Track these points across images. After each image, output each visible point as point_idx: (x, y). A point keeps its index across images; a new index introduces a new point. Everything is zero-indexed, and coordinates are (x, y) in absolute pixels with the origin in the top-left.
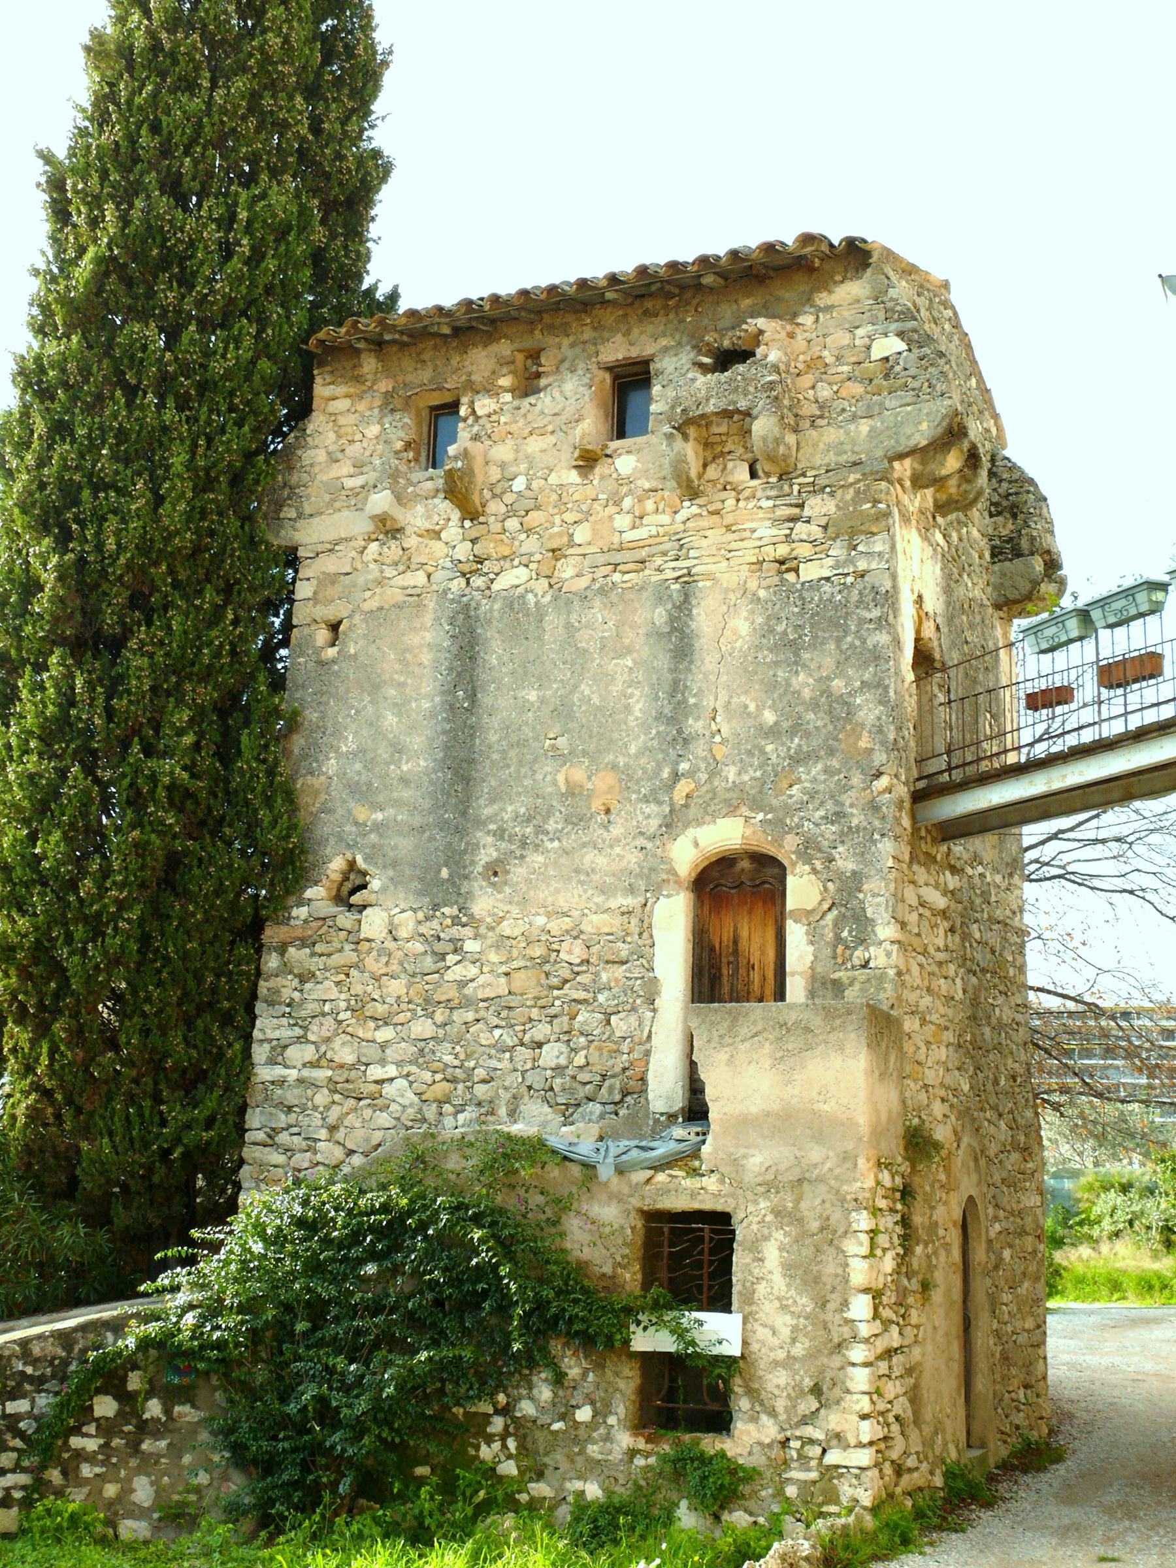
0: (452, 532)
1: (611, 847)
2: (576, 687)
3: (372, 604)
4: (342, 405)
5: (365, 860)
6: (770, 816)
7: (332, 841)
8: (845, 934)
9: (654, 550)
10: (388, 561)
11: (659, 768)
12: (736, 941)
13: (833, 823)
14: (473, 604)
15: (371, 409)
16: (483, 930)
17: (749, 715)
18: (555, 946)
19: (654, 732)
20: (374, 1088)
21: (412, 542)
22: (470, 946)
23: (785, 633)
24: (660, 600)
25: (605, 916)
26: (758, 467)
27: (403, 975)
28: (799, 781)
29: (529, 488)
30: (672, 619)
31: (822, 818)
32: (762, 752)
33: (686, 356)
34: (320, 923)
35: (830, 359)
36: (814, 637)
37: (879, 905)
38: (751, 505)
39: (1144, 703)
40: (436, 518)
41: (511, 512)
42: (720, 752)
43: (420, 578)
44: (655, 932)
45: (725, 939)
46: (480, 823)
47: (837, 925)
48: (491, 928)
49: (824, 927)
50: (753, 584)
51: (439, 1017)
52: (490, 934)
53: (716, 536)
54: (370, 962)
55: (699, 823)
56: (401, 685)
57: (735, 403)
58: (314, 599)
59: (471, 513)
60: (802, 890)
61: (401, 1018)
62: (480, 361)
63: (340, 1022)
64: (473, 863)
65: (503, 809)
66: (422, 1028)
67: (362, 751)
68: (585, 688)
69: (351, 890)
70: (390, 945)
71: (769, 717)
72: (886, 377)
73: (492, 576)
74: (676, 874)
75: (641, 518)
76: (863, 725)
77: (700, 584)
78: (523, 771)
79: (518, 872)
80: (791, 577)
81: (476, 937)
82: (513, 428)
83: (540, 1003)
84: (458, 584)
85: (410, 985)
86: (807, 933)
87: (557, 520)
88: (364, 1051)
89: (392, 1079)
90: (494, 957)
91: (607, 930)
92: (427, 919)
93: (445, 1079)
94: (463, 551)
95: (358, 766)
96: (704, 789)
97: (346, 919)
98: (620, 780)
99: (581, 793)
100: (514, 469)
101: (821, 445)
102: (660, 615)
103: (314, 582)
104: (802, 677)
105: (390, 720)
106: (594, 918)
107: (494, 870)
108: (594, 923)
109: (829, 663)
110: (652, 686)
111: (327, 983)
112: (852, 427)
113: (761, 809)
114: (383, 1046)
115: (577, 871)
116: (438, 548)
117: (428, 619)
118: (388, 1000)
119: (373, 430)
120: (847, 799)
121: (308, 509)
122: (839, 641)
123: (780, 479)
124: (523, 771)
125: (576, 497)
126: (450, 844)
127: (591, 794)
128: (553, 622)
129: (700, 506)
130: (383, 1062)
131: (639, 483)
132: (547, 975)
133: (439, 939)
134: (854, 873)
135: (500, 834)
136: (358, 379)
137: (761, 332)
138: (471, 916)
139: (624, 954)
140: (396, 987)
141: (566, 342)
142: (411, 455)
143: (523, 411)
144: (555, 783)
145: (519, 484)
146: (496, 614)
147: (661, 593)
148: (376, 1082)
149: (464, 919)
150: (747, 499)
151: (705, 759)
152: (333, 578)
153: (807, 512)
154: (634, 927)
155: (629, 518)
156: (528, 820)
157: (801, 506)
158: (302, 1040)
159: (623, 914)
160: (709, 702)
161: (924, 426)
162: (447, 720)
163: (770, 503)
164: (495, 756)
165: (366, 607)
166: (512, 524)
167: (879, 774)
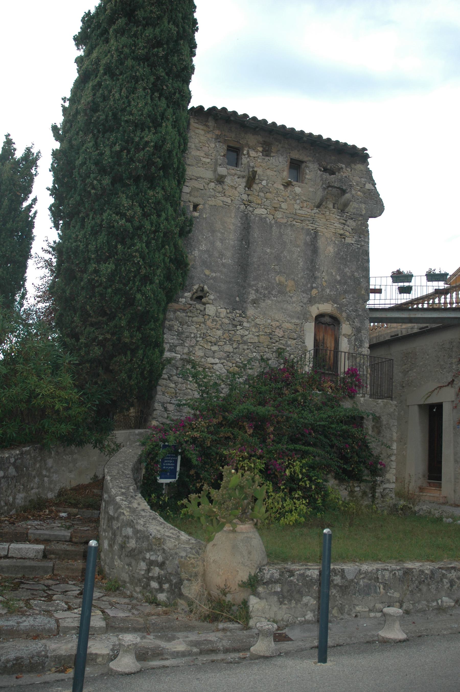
7: (196, 279)
9: (306, 219)
10: (217, 191)
12: (323, 339)
21: (226, 187)
22: (245, 324)
28: (346, 298)
29: (267, 185)
30: (312, 241)
33: (316, 166)
36: (350, 259)
41: (261, 190)
42: (324, 284)
46: (250, 286)
47: (356, 340)
50: (334, 239)
51: (235, 346)
53: (323, 220)
54: (209, 323)
55: (319, 303)
58: (190, 193)
60: (346, 328)
62: (252, 139)
63: (197, 341)
64: (247, 298)
66: (228, 348)
68: (285, 253)
69: (200, 297)
72: (369, 194)
79: (263, 305)
80: (343, 240)
81: (248, 322)
84: (243, 207)
85: (224, 334)
89: (216, 364)
90: (254, 330)
92: (230, 312)
97: (199, 306)
102: (308, 238)
105: (218, 244)
106: (286, 324)
107: (254, 302)
108: (286, 325)
110: (306, 259)
111: (193, 327)
114: (214, 352)
115: (282, 308)
117: (233, 215)
127: (286, 286)
130: (214, 358)
131: (302, 197)
132: (271, 338)
133: (234, 319)
135: (257, 291)
136: (207, 126)
137: (342, 168)
138: (246, 315)
139: (296, 337)
143: (266, 160)
144: (275, 279)
145: (264, 183)
147: (308, 232)
148: (211, 364)
158: (182, 345)
160: (322, 268)
162: (240, 250)
163: (339, 217)
164: (255, 266)
165: (210, 203)
166: (262, 194)
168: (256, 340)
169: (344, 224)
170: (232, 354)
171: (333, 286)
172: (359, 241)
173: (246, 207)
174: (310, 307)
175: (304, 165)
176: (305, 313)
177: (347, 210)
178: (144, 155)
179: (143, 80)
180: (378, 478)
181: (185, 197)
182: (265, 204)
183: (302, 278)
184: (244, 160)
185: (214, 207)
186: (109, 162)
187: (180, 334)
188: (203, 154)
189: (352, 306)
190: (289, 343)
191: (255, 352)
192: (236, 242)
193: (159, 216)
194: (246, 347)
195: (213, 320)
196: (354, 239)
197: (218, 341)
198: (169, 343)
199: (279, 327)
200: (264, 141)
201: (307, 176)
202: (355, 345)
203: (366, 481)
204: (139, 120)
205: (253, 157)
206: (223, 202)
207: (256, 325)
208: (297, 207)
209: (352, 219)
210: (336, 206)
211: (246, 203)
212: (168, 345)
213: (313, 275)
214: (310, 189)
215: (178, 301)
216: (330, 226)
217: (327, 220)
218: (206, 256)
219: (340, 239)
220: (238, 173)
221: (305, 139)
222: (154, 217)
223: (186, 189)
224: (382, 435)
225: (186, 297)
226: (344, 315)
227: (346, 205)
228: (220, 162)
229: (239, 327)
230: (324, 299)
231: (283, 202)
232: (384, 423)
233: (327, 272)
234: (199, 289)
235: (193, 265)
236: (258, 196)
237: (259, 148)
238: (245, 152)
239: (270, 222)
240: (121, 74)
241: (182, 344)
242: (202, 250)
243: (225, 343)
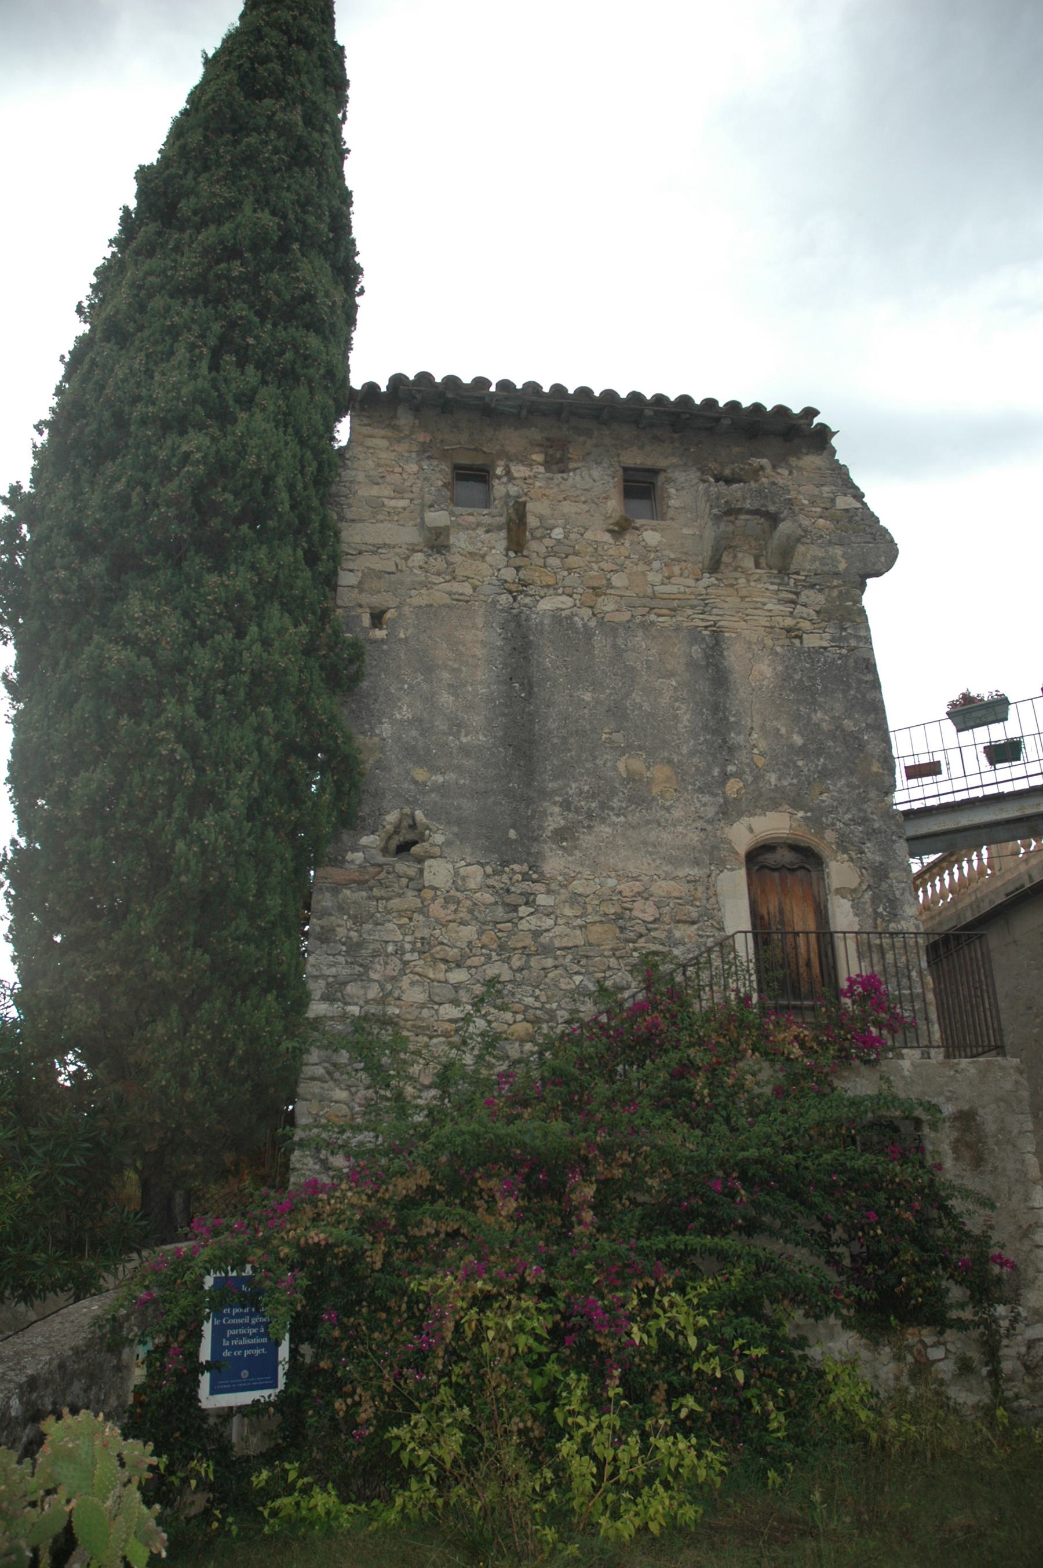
1: (675, 826)
3: (416, 601)
5: (426, 815)
7: (389, 796)
8: (880, 910)
9: (683, 603)
12: (781, 911)
13: (859, 824)
20: (448, 1026)
21: (457, 559)
22: (542, 900)
23: (801, 681)
27: (474, 922)
28: (828, 790)
30: (707, 657)
32: (795, 763)
33: (694, 475)
34: (377, 869)
36: (825, 687)
37: (904, 889)
39: (1010, 778)
40: (480, 545)
41: (551, 552)
42: (761, 762)
43: (467, 589)
44: (720, 898)
45: (771, 909)
46: (544, 794)
47: (875, 900)
50: (769, 642)
51: (516, 962)
53: (733, 601)
54: (436, 909)
56: (455, 671)
58: (360, 587)
59: (517, 544)
60: (840, 872)
61: (475, 961)
62: (512, 439)
63: (406, 963)
64: (541, 828)
68: (636, 697)
72: (850, 521)
74: (737, 853)
75: (669, 578)
79: (587, 840)
80: (797, 642)
81: (549, 892)
82: (547, 492)
83: (618, 953)
84: (505, 599)
85: (481, 933)
86: (852, 907)
88: (437, 990)
90: (568, 912)
91: (676, 894)
92: (495, 873)
93: (525, 1020)
97: (405, 867)
98: (677, 773)
99: (640, 780)
102: (696, 651)
103: (360, 574)
104: (819, 714)
105: (446, 699)
106: (663, 883)
107: (561, 835)
108: (661, 888)
111: (390, 926)
113: (801, 808)
114: (457, 987)
115: (645, 843)
116: (484, 567)
117: (480, 621)
121: (349, 514)
123: (780, 572)
127: (650, 781)
128: (600, 643)
131: (666, 553)
132: (622, 929)
133: (508, 891)
134: (881, 864)
135: (566, 805)
136: (395, 428)
138: (542, 874)
139: (694, 915)
140: (469, 932)
143: (555, 481)
144: (615, 768)
145: (558, 533)
147: (694, 636)
149: (535, 876)
151: (748, 765)
152: (380, 574)
153: (803, 598)
157: (797, 594)
158: (362, 978)
163: (776, 587)
164: (555, 740)
166: (554, 562)
168: (578, 938)
169: (794, 602)
170: (509, 987)
171: (785, 764)
172: (841, 638)
173: (515, 599)
174: (726, 830)
175: (661, 478)
176: (714, 847)
177: (793, 568)
178: (180, 487)
179: (189, 330)
180: (1001, 1310)
181: (345, 597)
182: (567, 582)
183: (692, 754)
184: (499, 489)
185: (429, 610)
186: (98, 522)
187: (354, 948)
188: (387, 491)
190: (677, 934)
191: (577, 973)
192: (494, 687)
193: (240, 634)
194: (549, 962)
195: (447, 900)
196: (827, 636)
197: (464, 957)
198: (325, 977)
199: (644, 895)
200: (548, 439)
201: (672, 503)
202: (877, 914)
203: (961, 1325)
204: (169, 411)
205: (522, 476)
206: (450, 593)
207: (575, 898)
208: (651, 577)
209: (812, 586)
210: (762, 561)
211: (513, 587)
212: (322, 983)
213: (724, 741)
214: (685, 531)
215: (344, 861)
216: (753, 614)
217: (743, 598)
218: (414, 733)
219: (787, 642)
220: (487, 520)
221: (648, 412)
222: (225, 639)
223: (346, 579)
224: (989, 1167)
225: (364, 848)
226: (830, 835)
227: (786, 553)
228: (429, 499)
229: (523, 910)
231: (617, 571)
232: (991, 1127)
233: (761, 730)
234: (405, 824)
235: (379, 761)
236: (545, 566)
237: (534, 457)
238: (499, 471)
239: (584, 625)
240: (141, 328)
241: (360, 975)
242: (401, 721)
243: (489, 958)
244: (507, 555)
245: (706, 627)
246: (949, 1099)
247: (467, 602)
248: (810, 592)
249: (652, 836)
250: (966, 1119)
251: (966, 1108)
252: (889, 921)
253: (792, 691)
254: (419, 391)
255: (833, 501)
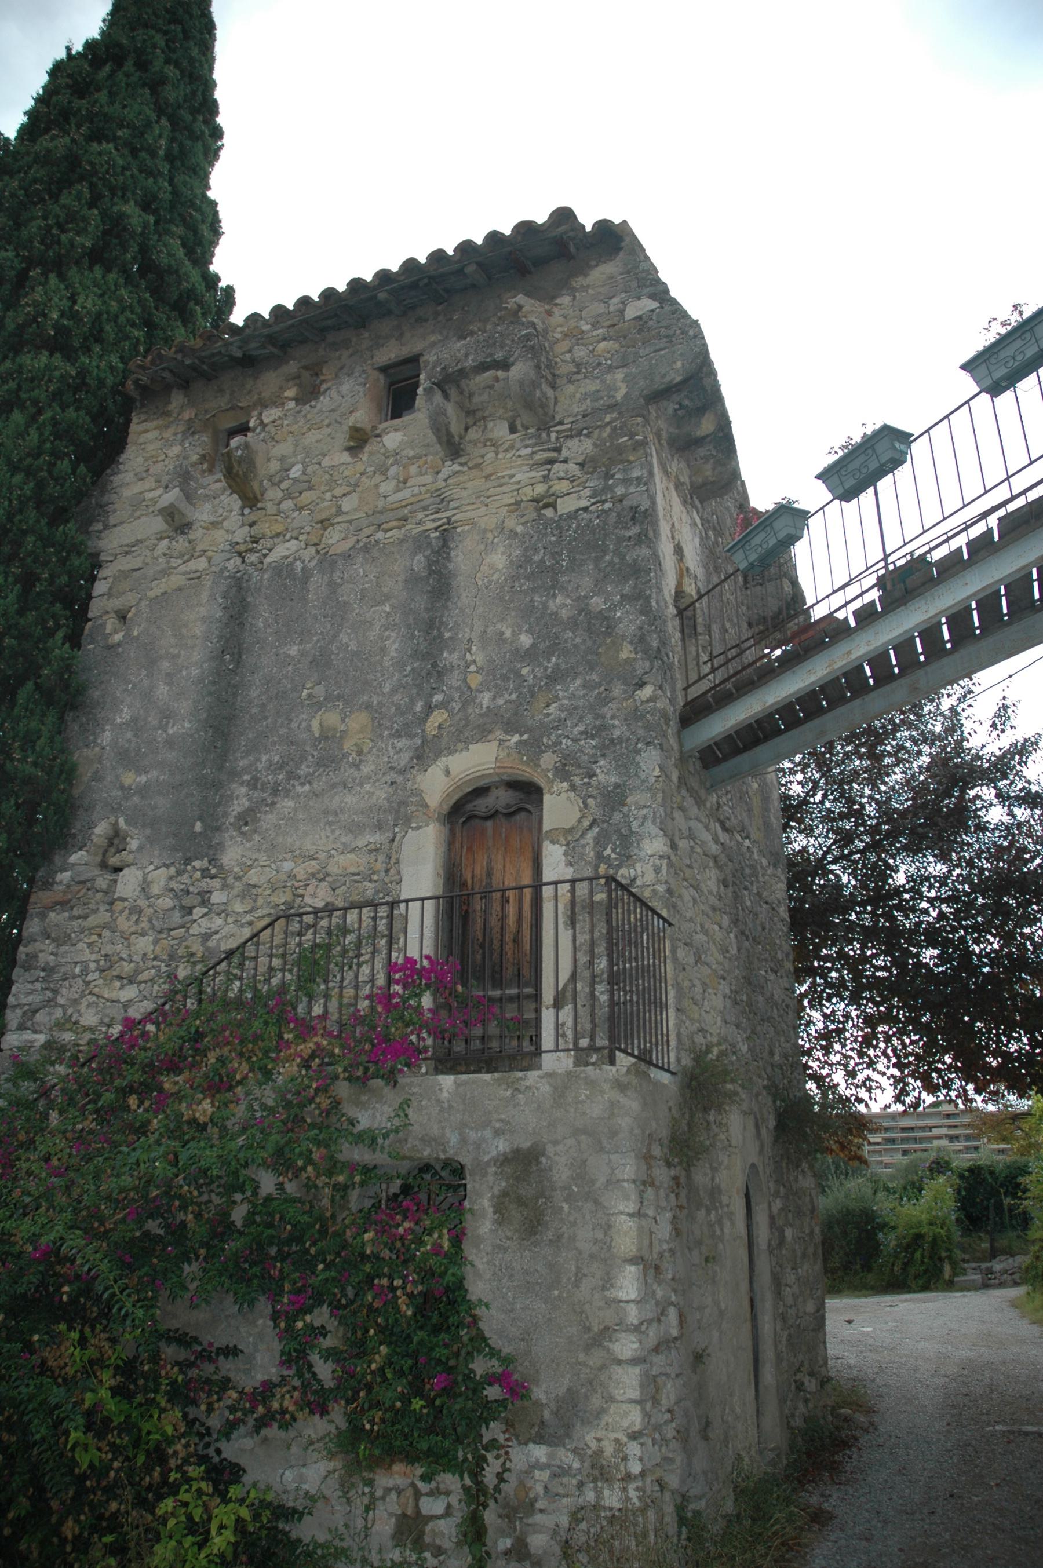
0: (234, 520)
1: (361, 785)
2: (335, 636)
3: (157, 591)
4: (152, 435)
5: (126, 821)
6: (525, 737)
7: (98, 808)
8: (608, 851)
10: (176, 554)
11: (412, 702)
14: (246, 577)
15: (175, 434)
16: (230, 880)
17: (505, 641)
18: (300, 891)
19: (409, 668)
22: (218, 897)
23: (542, 561)
24: (418, 548)
25: (351, 856)
26: (518, 423)
27: (150, 932)
28: (557, 698)
29: (304, 473)
30: (430, 563)
31: (581, 733)
32: (518, 674)
35: (586, 327)
36: (572, 561)
37: (645, 818)
38: (509, 455)
40: (220, 511)
41: (288, 495)
43: (201, 564)
45: (478, 871)
46: (234, 775)
47: (600, 843)
48: (238, 878)
49: (584, 846)
52: (237, 884)
54: (124, 923)
55: (451, 752)
57: (491, 355)
58: (109, 594)
59: (251, 500)
60: (558, 808)
62: (270, 381)
64: (226, 815)
65: (258, 760)
67: (134, 720)
68: (343, 638)
70: (142, 903)
71: (526, 640)
72: (640, 331)
73: (265, 552)
74: (427, 806)
75: (405, 482)
76: (623, 637)
77: (459, 530)
78: (280, 721)
79: (268, 819)
80: (549, 513)
81: (225, 887)
85: (156, 942)
86: (565, 854)
87: (328, 495)
90: (238, 907)
91: (353, 870)
92: (179, 873)
94: (242, 534)
95: (129, 735)
96: (457, 718)
98: (373, 719)
99: (334, 736)
100: (293, 460)
101: (578, 395)
102: (419, 563)
104: (559, 600)
105: (162, 690)
107: (247, 818)
109: (587, 582)
110: (409, 626)
112: (609, 377)
113: (516, 730)
115: (326, 812)
116: (220, 535)
117: (204, 597)
118: (135, 958)
119: (176, 450)
120: (607, 711)
122: (597, 560)
124: (280, 721)
125: (347, 473)
126: (206, 797)
128: (317, 582)
129: (461, 465)
133: (188, 892)
134: (617, 786)
135: (253, 784)
138: (221, 867)
140: (144, 944)
141: (346, 353)
142: (205, 466)
144: (309, 728)
145: (295, 472)
146: (265, 583)
147: (420, 542)
149: (214, 871)
150: (506, 451)
151: (458, 689)
152: (125, 575)
153: (565, 453)
154: (380, 866)
155: (394, 483)
156: (281, 768)
157: (558, 450)
159: (371, 851)
160: (465, 633)
161: (679, 364)
163: (529, 450)
164: (254, 710)
165: (151, 594)
166: (287, 505)
167: (641, 685)
176: (403, 803)
183: (394, 691)
189: (581, 719)
197: (137, 972)
213: (434, 665)
215: (54, 883)
224: (550, 1234)
226: (548, 760)
230: (464, 734)
232: (561, 1174)
235: (96, 772)
244: (243, 514)
245: (436, 529)
246: (498, 1133)
247: (199, 578)
248: (570, 443)
249: (335, 803)
250: (524, 1162)
251: (526, 1144)
252: (619, 866)
253: (527, 578)
254: (163, 369)
255: (622, 312)
